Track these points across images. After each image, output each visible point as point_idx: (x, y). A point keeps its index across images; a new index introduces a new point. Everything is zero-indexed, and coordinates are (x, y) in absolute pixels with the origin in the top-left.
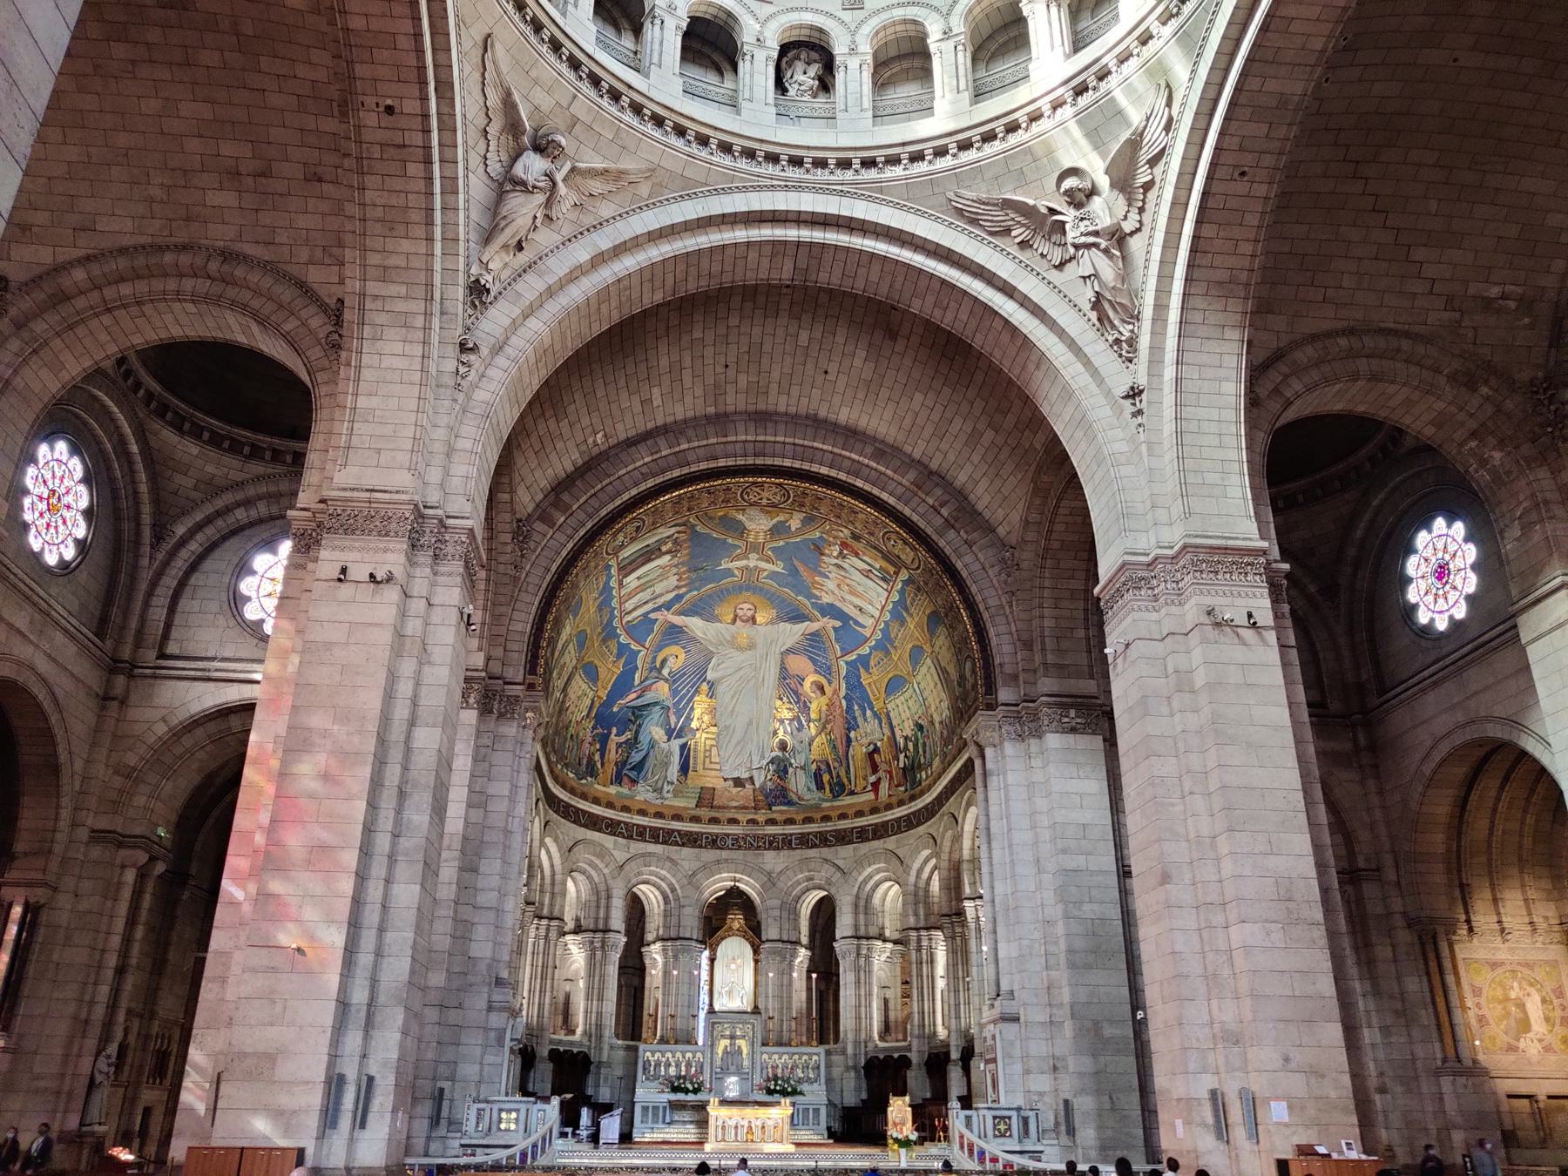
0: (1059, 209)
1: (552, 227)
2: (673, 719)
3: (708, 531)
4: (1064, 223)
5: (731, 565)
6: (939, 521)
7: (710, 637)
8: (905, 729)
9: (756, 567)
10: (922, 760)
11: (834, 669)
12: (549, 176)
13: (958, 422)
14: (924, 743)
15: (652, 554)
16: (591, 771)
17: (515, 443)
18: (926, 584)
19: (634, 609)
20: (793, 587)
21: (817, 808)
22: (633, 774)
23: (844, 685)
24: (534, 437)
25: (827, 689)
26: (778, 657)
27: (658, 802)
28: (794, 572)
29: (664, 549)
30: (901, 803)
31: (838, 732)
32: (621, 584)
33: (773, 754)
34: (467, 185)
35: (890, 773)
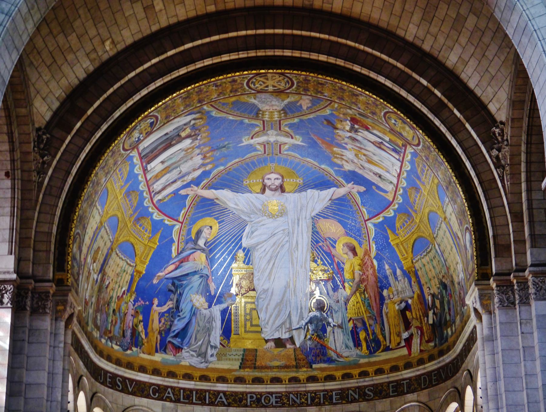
2: (212, 286)
3: (224, 115)
5: (252, 141)
7: (241, 207)
9: (276, 142)
11: (364, 231)
13: (443, 7)
15: (172, 139)
16: (136, 341)
17: (27, 62)
18: (427, 159)
19: (164, 189)
20: (315, 157)
21: (356, 365)
22: (176, 341)
23: (374, 246)
24: (45, 54)
25: (358, 250)
26: (309, 221)
27: (203, 366)
28: (313, 144)
29: (183, 134)
30: (431, 358)
31: (371, 292)
32: (145, 170)
33: (312, 314)
35: (420, 328)
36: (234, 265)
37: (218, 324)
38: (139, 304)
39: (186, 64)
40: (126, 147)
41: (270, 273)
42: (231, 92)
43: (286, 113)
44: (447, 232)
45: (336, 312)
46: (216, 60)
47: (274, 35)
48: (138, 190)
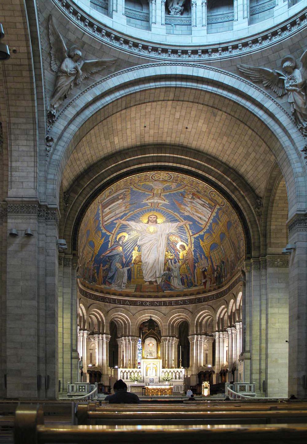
0: (282, 74)
1: (78, 87)
2: (124, 260)
4: (284, 80)
6: (232, 188)
8: (216, 263)
10: (223, 275)
12: (76, 68)
14: (224, 269)
22: (110, 281)
29: (120, 197)
32: (103, 212)
33: (165, 272)
34: (44, 76)
36: (134, 252)
37: (126, 274)
38: (95, 265)
39: (127, 167)
40: (99, 202)
41: (148, 255)
42: (144, 180)
43: (164, 190)
44: (229, 242)
45: (175, 272)
46: (140, 166)
47: (165, 156)
48: (99, 219)
